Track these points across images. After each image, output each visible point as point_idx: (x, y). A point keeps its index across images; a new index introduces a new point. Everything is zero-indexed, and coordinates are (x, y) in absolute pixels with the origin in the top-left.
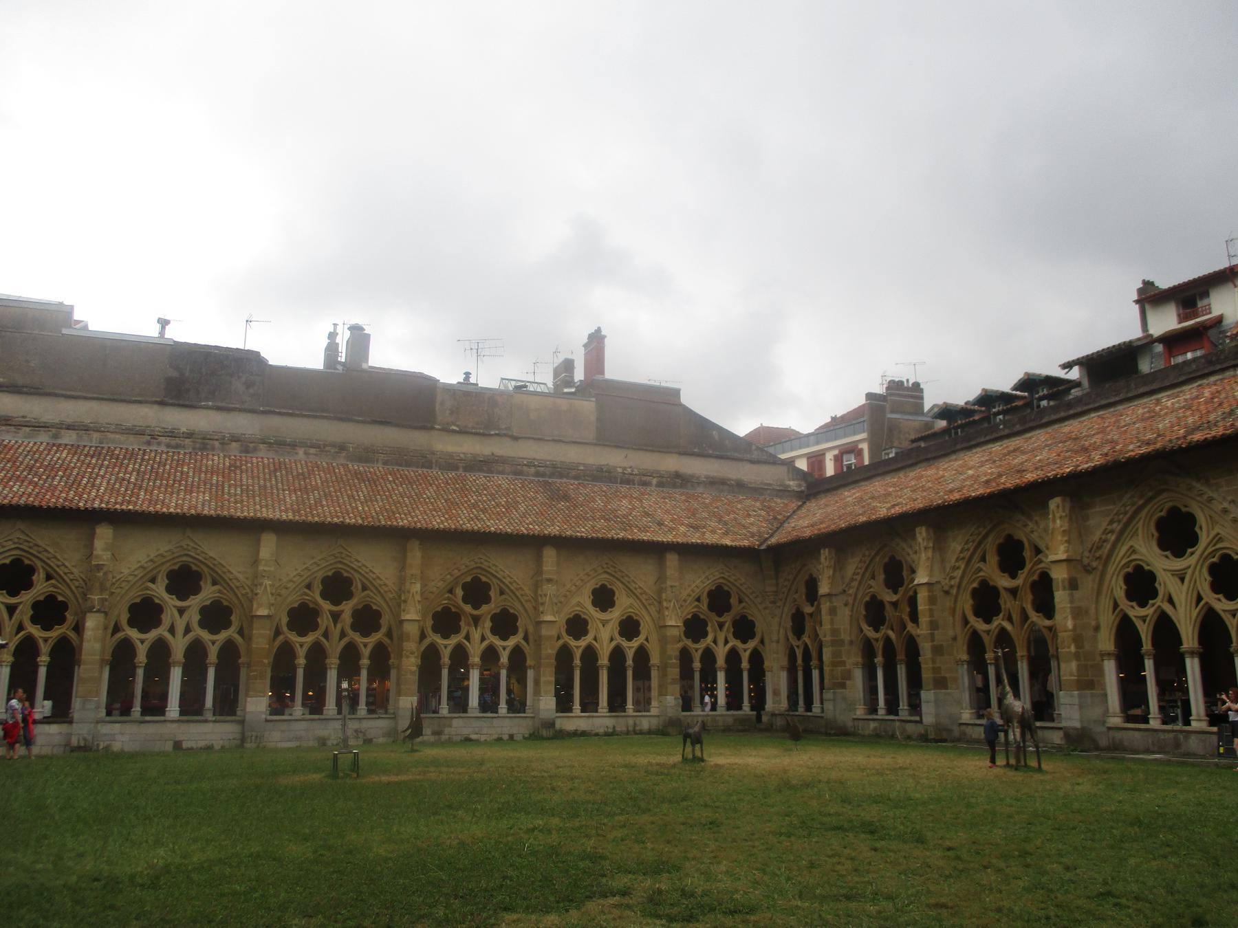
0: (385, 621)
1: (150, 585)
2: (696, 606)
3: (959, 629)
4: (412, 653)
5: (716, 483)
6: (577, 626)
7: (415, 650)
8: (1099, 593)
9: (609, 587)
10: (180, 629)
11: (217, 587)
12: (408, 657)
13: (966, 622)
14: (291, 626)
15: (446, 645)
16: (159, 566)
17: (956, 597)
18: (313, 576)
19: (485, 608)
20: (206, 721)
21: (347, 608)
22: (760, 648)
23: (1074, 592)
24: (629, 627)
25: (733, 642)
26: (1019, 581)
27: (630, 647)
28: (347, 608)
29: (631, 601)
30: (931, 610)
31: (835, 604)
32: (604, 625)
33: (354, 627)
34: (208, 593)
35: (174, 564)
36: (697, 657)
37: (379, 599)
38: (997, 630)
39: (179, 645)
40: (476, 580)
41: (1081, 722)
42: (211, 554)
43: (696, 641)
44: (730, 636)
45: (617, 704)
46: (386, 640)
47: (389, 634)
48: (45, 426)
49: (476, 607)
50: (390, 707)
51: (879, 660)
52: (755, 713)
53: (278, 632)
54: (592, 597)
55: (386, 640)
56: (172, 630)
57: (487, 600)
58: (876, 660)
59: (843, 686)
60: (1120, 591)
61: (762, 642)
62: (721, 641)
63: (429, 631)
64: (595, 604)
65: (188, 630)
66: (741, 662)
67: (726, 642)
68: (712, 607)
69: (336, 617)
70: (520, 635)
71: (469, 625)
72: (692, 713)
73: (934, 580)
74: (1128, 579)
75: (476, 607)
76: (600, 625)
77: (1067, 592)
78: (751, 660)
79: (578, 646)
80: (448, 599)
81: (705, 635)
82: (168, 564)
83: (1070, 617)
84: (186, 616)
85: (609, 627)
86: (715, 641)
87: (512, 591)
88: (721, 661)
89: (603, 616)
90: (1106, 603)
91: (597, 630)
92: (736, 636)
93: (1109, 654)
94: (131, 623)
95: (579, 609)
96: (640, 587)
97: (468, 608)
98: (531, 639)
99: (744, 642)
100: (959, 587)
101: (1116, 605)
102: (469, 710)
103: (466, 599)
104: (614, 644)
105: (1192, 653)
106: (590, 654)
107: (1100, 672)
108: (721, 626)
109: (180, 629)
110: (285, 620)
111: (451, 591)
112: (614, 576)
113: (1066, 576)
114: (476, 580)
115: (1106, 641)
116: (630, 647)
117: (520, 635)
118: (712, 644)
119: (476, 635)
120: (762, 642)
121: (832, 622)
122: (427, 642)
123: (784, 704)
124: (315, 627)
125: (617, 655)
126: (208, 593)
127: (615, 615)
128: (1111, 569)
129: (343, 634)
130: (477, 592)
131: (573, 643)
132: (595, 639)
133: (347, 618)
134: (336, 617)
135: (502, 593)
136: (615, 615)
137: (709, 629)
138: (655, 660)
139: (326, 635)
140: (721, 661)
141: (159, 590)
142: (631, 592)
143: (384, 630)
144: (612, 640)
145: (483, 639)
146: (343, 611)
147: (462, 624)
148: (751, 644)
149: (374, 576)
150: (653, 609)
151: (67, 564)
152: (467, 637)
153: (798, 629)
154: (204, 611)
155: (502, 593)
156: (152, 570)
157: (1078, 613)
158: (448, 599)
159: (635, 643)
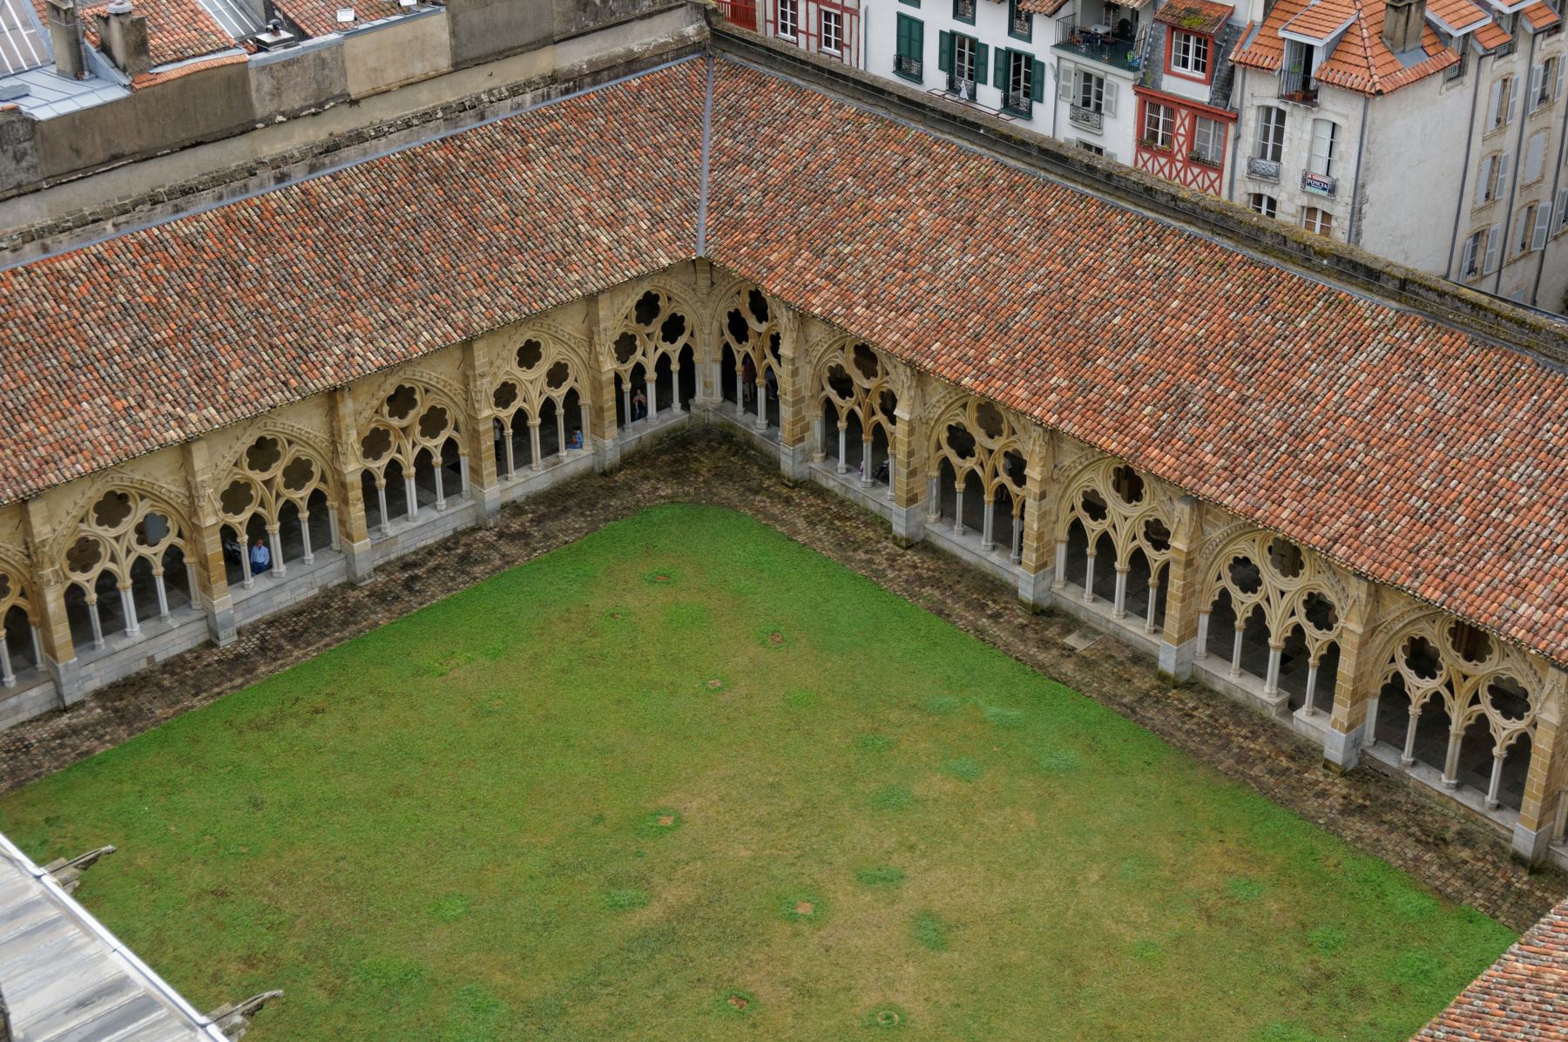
3: (932, 450)
5: (597, 73)
8: (1062, 497)
13: (939, 447)
24: (557, 375)
28: (277, 471)
29: (560, 348)
42: (138, 476)
45: (550, 449)
55: (322, 487)
56: (113, 559)
60: (1079, 502)
61: (692, 335)
78: (681, 359)
90: (1066, 505)
91: (527, 391)
97: (395, 422)
98: (462, 428)
101: (1073, 509)
105: (1122, 572)
107: (1052, 552)
109: (121, 554)
115: (1062, 532)
123: (717, 396)
126: (140, 511)
128: (1074, 485)
129: (278, 496)
138: (585, 400)
143: (317, 476)
147: (392, 439)
150: (583, 352)
157: (1042, 516)
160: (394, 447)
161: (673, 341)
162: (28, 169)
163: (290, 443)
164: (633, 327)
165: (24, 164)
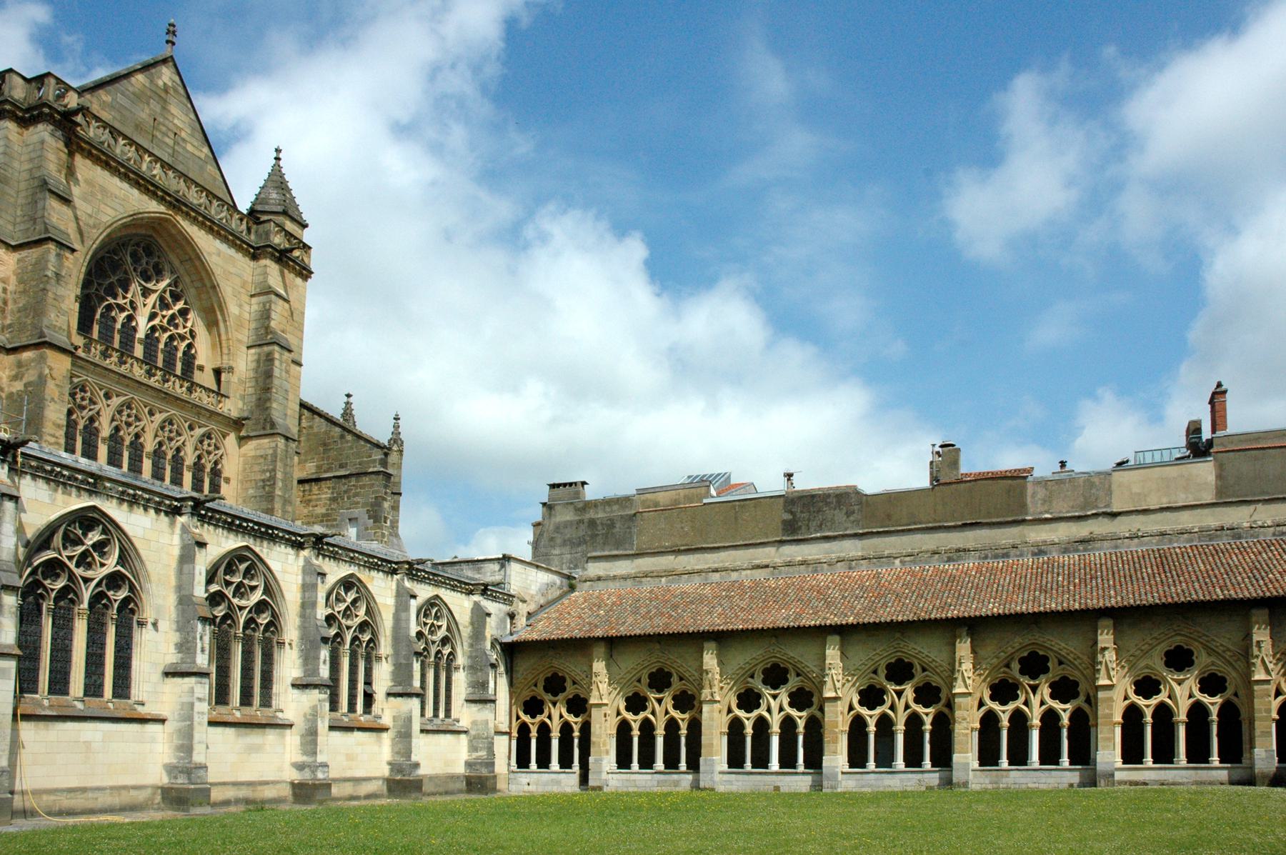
1: (750, 680)
9: (1186, 647)
15: (1004, 713)
16: (754, 666)
35: (767, 664)
37: (936, 678)
46: (946, 710)
48: (699, 572)
80: (1004, 672)
82: (762, 664)
87: (1070, 661)
95: (1147, 671)
96: (1222, 645)
112: (1190, 637)
135: (1061, 663)
142: (1211, 651)
143: (943, 701)
149: (930, 660)
151: (690, 669)
155: (1061, 663)
156: (749, 670)
158: (1004, 672)
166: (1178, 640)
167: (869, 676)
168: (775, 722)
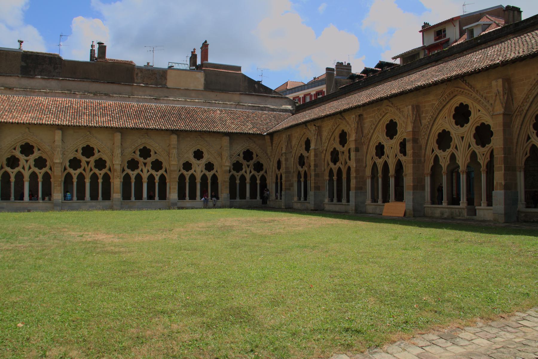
0: (108, 164)
1: (14, 151)
2: (238, 158)
3: (326, 167)
4: (118, 177)
6: (187, 166)
7: (119, 176)
10: (27, 168)
11: (40, 152)
12: (116, 178)
14: (70, 166)
17: (325, 154)
18: (79, 146)
19: (148, 159)
20: (39, 202)
21: (92, 159)
22: (265, 175)
23: (357, 153)
24: (209, 166)
25: (253, 172)
26: (344, 149)
27: (209, 175)
30: (315, 160)
31: (287, 157)
32: (199, 166)
33: (96, 167)
34: (36, 154)
35: (23, 142)
36: (238, 178)
38: (337, 169)
39: (27, 174)
40: (145, 148)
41: (355, 202)
43: (238, 172)
44: (252, 170)
47: (110, 170)
49: (145, 158)
50: (111, 198)
51: (302, 180)
52: (261, 200)
53: (65, 169)
54: (193, 154)
56: (24, 168)
57: (150, 156)
58: (301, 179)
59: (289, 189)
62: (248, 172)
63: (126, 168)
64: (195, 157)
65: (30, 168)
66: (257, 180)
67: (251, 172)
68: (244, 158)
69: (88, 163)
70: (164, 169)
71: (142, 166)
72: (235, 200)
73: (317, 147)
74: (377, 148)
75: (145, 158)
76: (197, 166)
77: (354, 153)
79: (187, 174)
81: (242, 169)
82: (20, 142)
83: (354, 163)
84: (29, 162)
85: (201, 166)
86: (246, 172)
88: (248, 180)
89: (198, 162)
92: (255, 169)
93: (369, 177)
94: (8, 165)
99: (258, 172)
100: (326, 150)
102: (143, 199)
103: (141, 156)
104: (202, 173)
106: (193, 178)
107: (365, 183)
108: (248, 166)
109: (27, 168)
110: (68, 164)
111: (134, 152)
113: (354, 147)
114: (145, 148)
116: (209, 175)
117: (164, 169)
118: (245, 173)
119: (145, 170)
120: (266, 172)
121: (286, 164)
122: (125, 173)
124: (80, 167)
125: (204, 178)
126: (36, 154)
127: (203, 161)
128: (371, 144)
129: (91, 170)
130: (145, 153)
131: (185, 173)
132: (195, 171)
133: (92, 164)
134: (88, 163)
136: (203, 161)
137: (243, 167)
139: (84, 170)
140: (248, 180)
141: (18, 153)
144: (202, 171)
145: (148, 171)
146: (91, 160)
148: (261, 173)
149: (102, 147)
152: (142, 171)
153: (279, 167)
154: (36, 160)
156: (13, 145)
157: (358, 161)
159: (212, 173)
160: (140, 169)
161: (258, 172)
162: (57, 73)
163: (99, 152)
164: (241, 160)
165: (56, 71)
166: (198, 147)
167: (74, 153)
168: (27, 174)
